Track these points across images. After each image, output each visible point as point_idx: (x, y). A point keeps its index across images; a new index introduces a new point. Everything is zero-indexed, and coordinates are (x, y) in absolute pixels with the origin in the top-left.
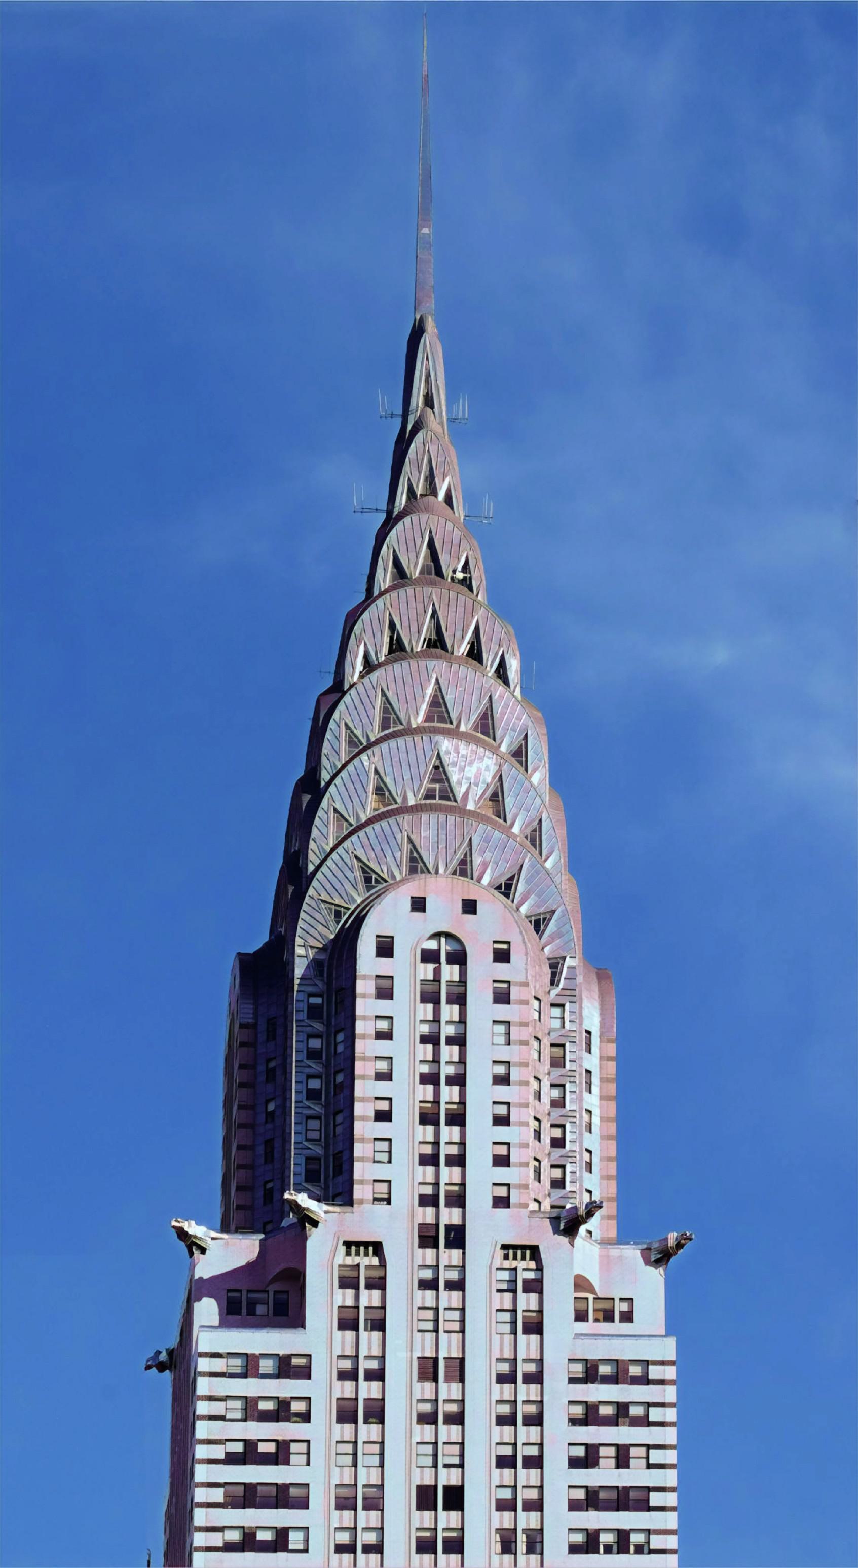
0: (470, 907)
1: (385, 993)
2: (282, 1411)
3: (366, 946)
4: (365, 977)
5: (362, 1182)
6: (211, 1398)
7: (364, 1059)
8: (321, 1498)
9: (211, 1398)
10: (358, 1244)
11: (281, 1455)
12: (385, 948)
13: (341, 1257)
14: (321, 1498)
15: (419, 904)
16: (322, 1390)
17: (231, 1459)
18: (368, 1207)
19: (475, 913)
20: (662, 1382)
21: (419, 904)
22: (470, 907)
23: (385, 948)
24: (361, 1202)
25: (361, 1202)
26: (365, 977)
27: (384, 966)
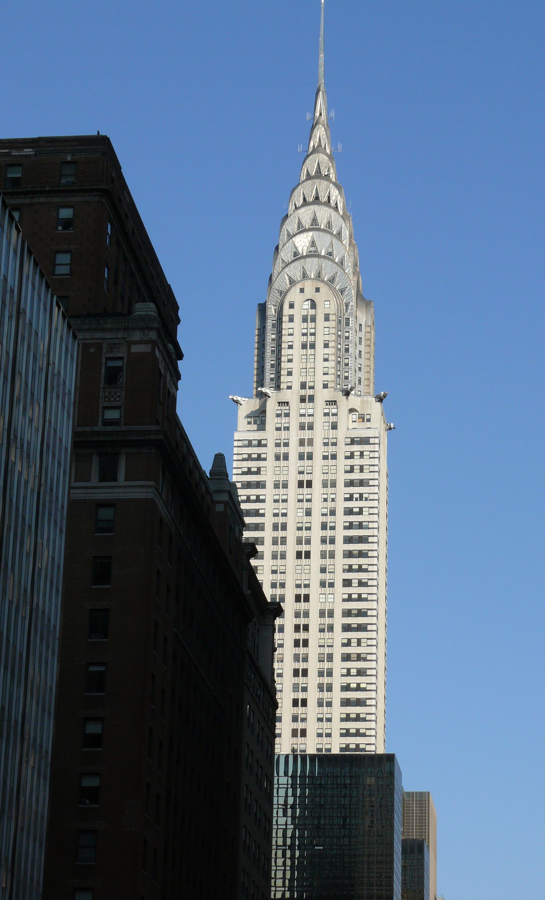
0: (318, 290)
1: (291, 319)
2: (259, 458)
3: (286, 306)
4: (285, 316)
5: (283, 383)
6: (238, 454)
7: (284, 342)
8: (270, 485)
9: (238, 454)
10: (282, 403)
11: (258, 472)
12: (292, 306)
13: (277, 407)
14: (270, 485)
15: (302, 291)
16: (270, 451)
17: (243, 473)
18: (285, 390)
19: (319, 292)
20: (374, 444)
21: (302, 291)
22: (318, 290)
23: (292, 306)
24: (283, 389)
25: (283, 389)
26: (285, 316)
27: (291, 312)
